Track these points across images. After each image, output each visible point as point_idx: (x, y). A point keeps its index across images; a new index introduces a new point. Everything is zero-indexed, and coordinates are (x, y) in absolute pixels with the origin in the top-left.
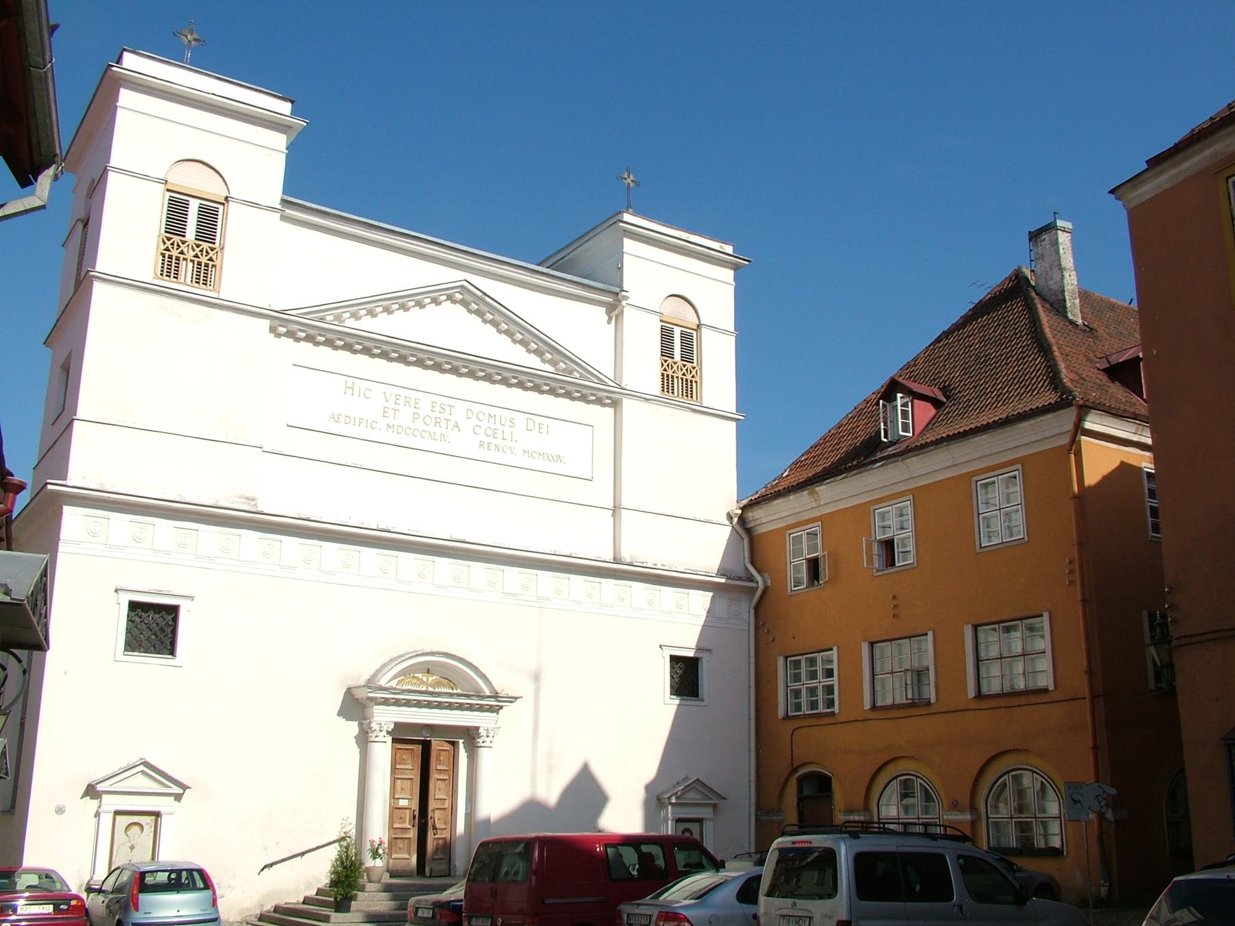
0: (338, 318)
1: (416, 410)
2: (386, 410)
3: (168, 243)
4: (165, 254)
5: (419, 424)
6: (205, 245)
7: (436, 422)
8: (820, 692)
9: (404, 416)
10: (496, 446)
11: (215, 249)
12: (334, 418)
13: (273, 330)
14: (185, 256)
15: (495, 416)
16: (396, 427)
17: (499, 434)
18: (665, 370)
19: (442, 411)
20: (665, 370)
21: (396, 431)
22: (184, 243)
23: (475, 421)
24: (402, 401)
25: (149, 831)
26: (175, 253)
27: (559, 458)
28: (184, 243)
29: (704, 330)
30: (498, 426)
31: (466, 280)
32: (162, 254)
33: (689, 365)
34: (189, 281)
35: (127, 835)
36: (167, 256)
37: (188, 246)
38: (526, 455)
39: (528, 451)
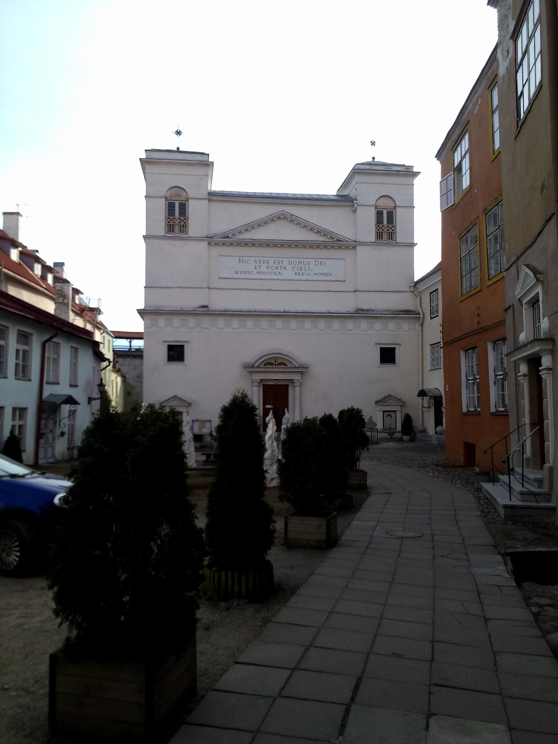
0: (234, 235)
5: (270, 270)
9: (263, 268)
10: (302, 273)
15: (301, 262)
19: (279, 263)
20: (378, 230)
21: (260, 274)
24: (262, 262)
29: (397, 209)
30: (303, 265)
31: (283, 211)
34: (178, 232)
39: (316, 274)
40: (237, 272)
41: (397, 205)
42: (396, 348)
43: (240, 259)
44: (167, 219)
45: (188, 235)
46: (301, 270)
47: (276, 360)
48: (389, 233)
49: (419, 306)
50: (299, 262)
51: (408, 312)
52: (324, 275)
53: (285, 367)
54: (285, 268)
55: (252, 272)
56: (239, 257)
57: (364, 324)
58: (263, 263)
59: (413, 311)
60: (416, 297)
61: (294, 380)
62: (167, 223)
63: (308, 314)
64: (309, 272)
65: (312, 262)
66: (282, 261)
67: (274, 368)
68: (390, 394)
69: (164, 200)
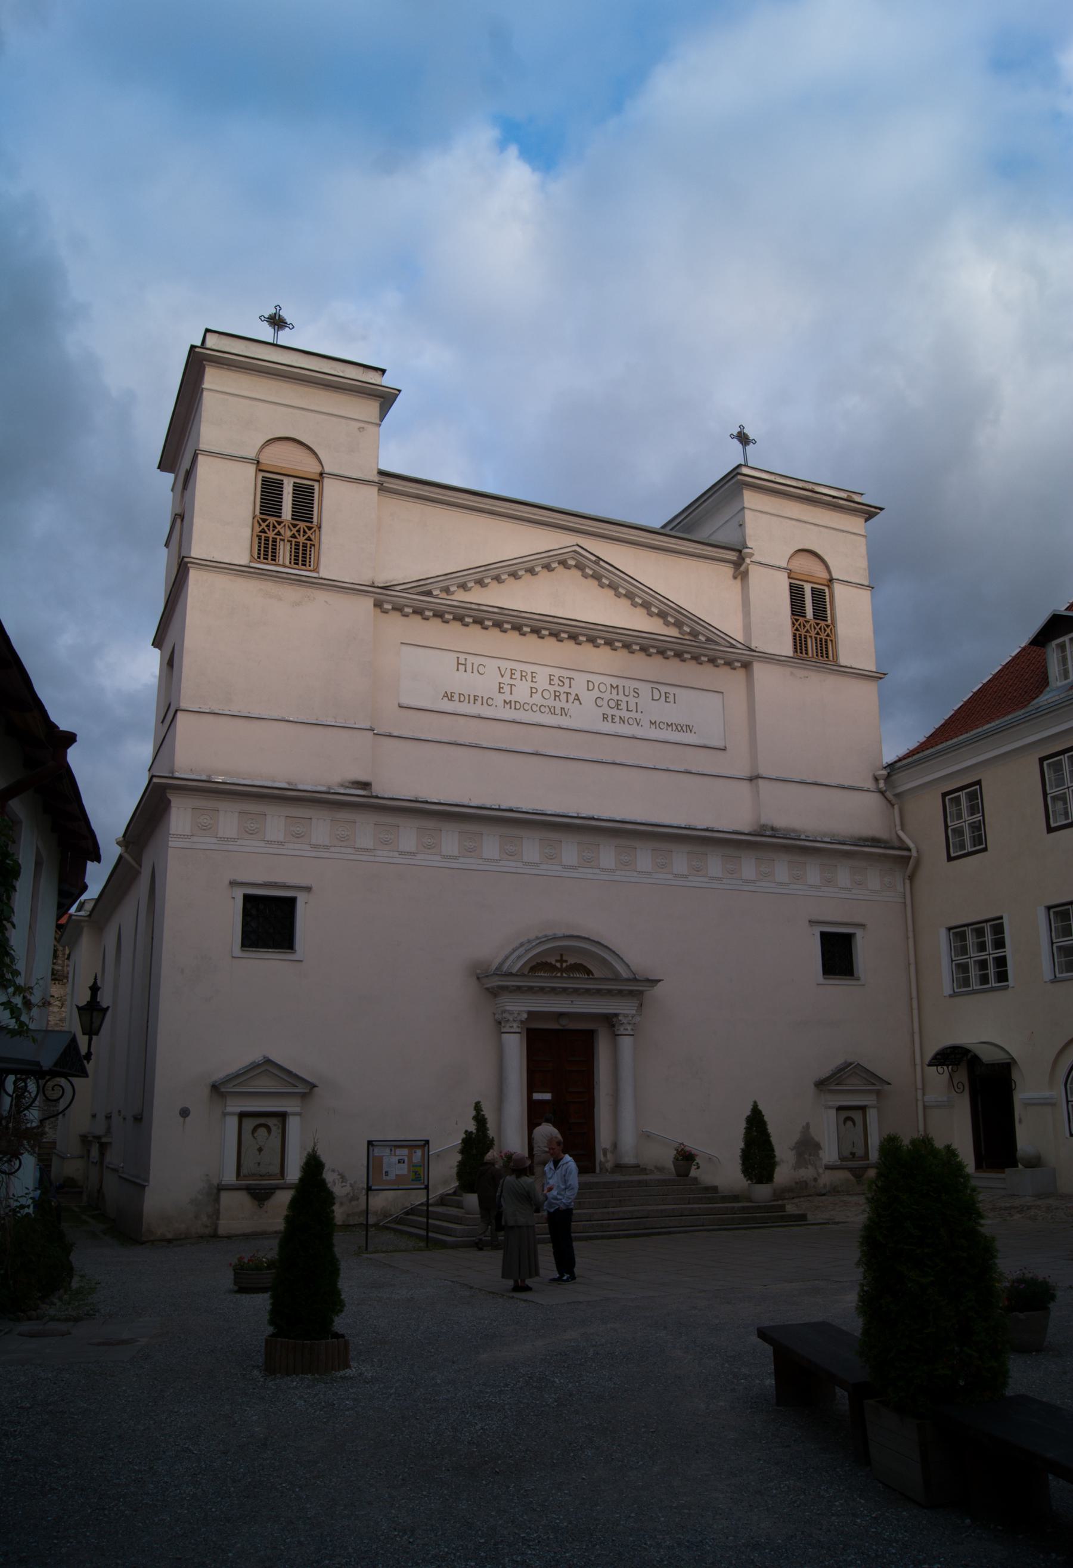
0: (446, 590)
1: (533, 685)
2: (502, 685)
3: (264, 525)
4: (261, 536)
6: (302, 525)
7: (555, 696)
8: (991, 964)
10: (620, 717)
11: (312, 528)
12: (447, 696)
13: (378, 605)
14: (281, 537)
15: (617, 686)
16: (513, 703)
17: (623, 706)
18: (797, 630)
19: (561, 684)
20: (797, 630)
22: (279, 523)
23: (596, 693)
24: (518, 675)
25: (276, 1131)
26: (271, 534)
27: (689, 728)
28: (279, 523)
30: (621, 697)
31: (578, 545)
32: (257, 536)
33: (823, 623)
34: (287, 563)
35: (254, 1137)
36: (263, 538)
37: (285, 526)
38: (653, 727)
39: (655, 722)
40: (451, 693)
41: (835, 576)
42: (857, 934)
43: (458, 658)
44: (258, 522)
45: (318, 572)
46: (618, 709)
47: (562, 955)
48: (821, 640)
49: (898, 828)
50: (611, 686)
51: (875, 842)
52: (674, 728)
53: (586, 976)
54: (577, 698)
55: (492, 699)
56: (459, 655)
57: (781, 869)
58: (521, 680)
59: (885, 842)
60: (889, 805)
61: (620, 1018)
62: (257, 529)
63: (650, 829)
64: (638, 716)
65: (645, 689)
66: (570, 678)
67: (558, 977)
68: (849, 1061)
69: (252, 469)
